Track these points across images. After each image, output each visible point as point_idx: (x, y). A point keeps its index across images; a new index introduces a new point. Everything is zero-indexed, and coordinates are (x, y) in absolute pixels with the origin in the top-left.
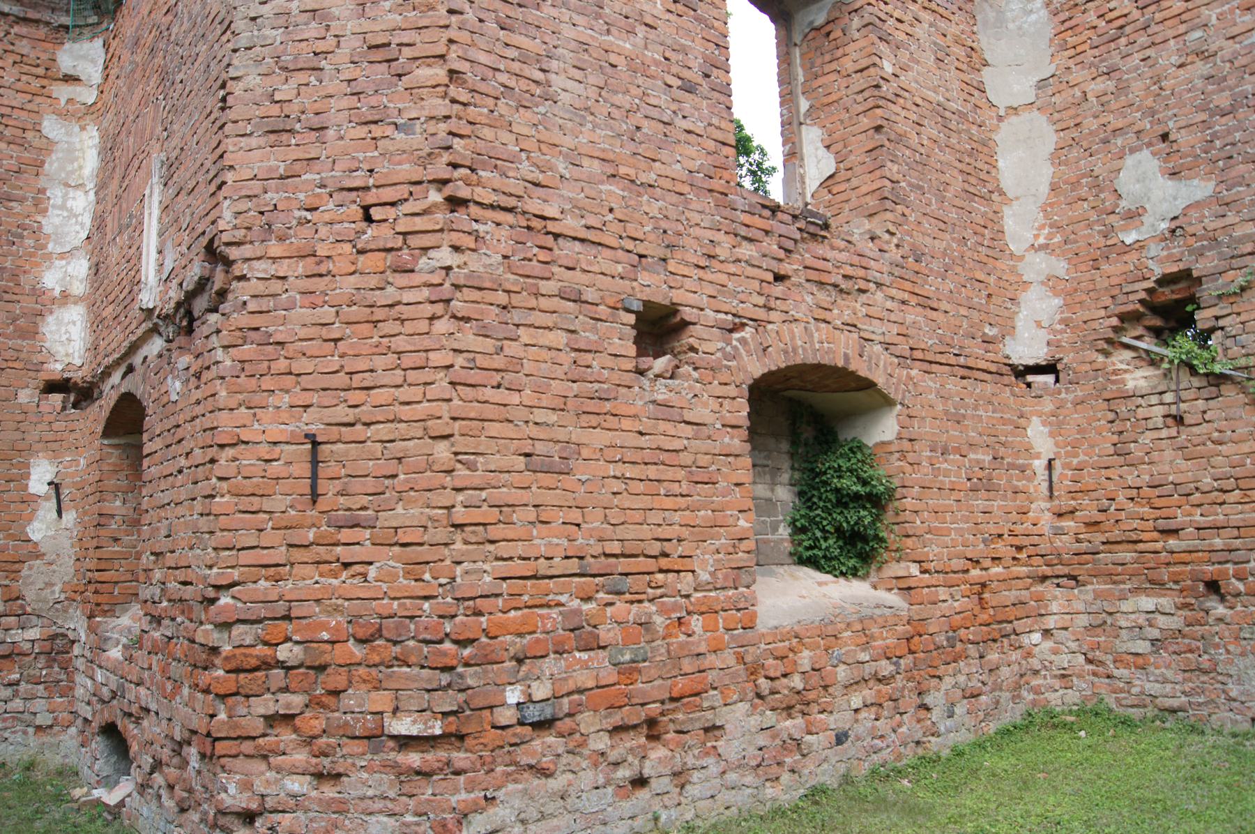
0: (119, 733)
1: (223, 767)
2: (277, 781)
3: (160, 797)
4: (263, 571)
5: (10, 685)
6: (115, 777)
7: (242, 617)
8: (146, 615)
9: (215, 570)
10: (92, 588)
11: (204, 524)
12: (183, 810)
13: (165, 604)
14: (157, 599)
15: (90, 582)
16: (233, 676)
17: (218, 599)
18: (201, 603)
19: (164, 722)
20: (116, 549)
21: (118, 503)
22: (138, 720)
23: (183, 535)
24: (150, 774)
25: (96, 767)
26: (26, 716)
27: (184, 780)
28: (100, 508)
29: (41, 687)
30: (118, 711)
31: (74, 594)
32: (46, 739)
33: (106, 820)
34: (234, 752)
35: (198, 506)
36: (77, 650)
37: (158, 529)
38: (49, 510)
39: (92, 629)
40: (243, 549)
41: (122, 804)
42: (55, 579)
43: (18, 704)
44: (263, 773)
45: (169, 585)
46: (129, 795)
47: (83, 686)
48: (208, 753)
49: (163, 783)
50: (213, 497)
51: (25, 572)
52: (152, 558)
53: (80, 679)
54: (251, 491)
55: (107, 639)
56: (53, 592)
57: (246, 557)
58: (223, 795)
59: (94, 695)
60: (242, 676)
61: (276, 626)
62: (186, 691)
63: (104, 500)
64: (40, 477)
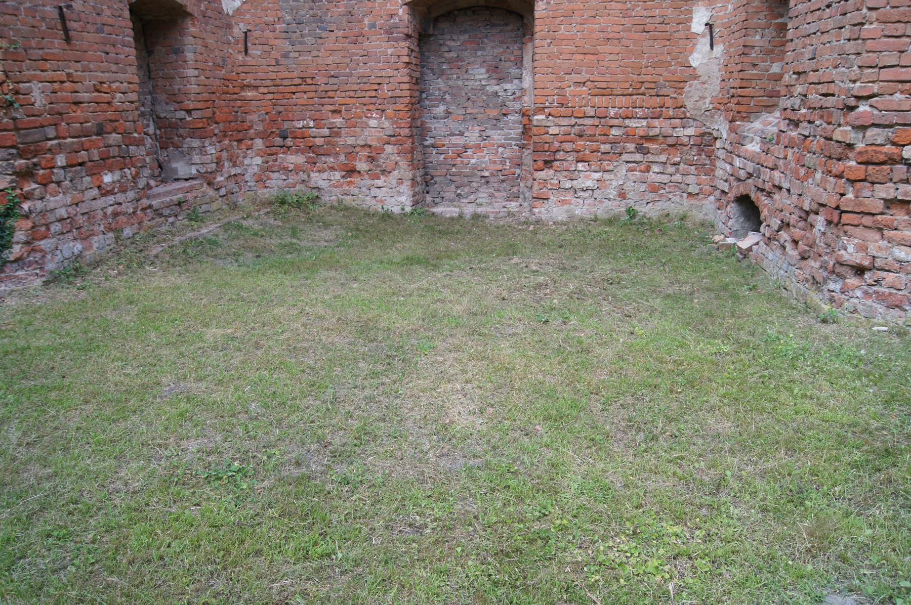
0: (753, 202)
1: (845, 232)
2: (887, 248)
3: (784, 248)
4: (900, 86)
5: (674, 164)
6: (741, 232)
7: (877, 122)
8: (785, 119)
9: (858, 84)
10: (735, 100)
11: (851, 47)
12: (803, 258)
13: (803, 111)
14: (796, 107)
15: (733, 96)
16: (863, 167)
17: (857, 107)
18: (842, 109)
19: (795, 197)
20: (754, 72)
21: (758, 37)
22: (769, 194)
23: (828, 57)
24: (778, 231)
25: (730, 223)
26: (683, 186)
27: (807, 238)
28: (745, 41)
29: (693, 168)
30: (753, 187)
31: (720, 105)
32: (694, 202)
33: (738, 257)
34: (856, 223)
35: (846, 33)
36: (718, 144)
37: (802, 54)
38: (705, 44)
39: (732, 130)
40: (885, 67)
41: (750, 249)
42: (707, 94)
43: (678, 177)
44: (877, 241)
45: (810, 97)
46: (757, 244)
47: (722, 169)
48: (836, 220)
49: (788, 238)
50: (863, 24)
51: (687, 89)
52: (795, 76)
53: (719, 164)
54: (897, 18)
55: (745, 137)
56: (705, 103)
57: (886, 74)
58: (843, 252)
59: (732, 175)
60: (870, 167)
61: (906, 130)
62: (818, 175)
63: (749, 35)
64: (699, 20)
